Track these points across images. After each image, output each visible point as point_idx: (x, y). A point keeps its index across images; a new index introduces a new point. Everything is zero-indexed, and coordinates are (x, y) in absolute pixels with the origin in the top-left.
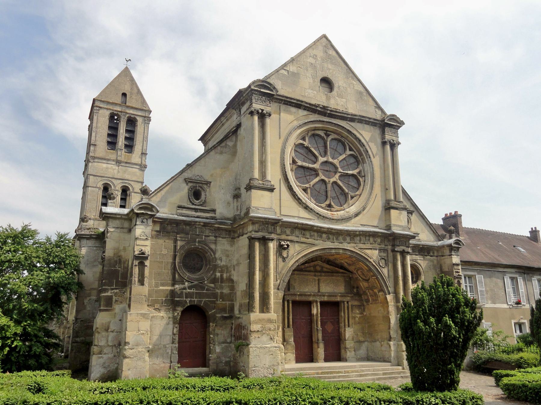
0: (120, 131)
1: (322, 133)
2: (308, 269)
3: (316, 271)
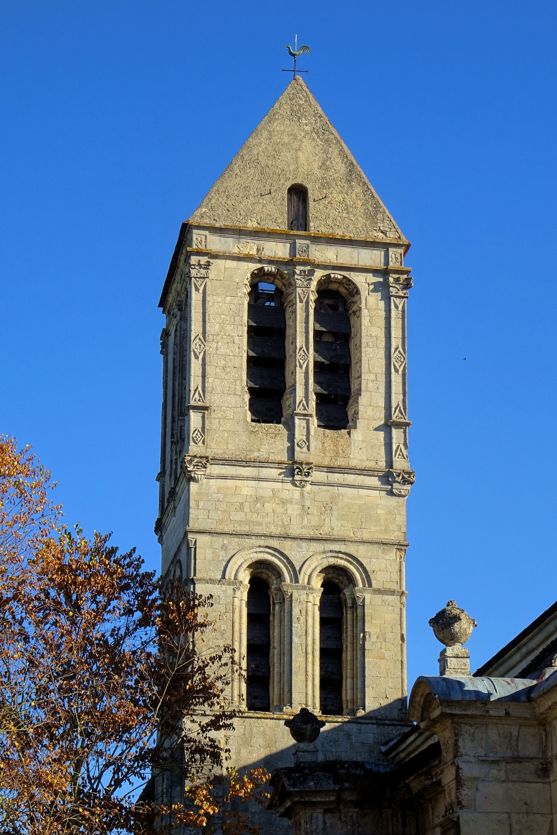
0: (294, 342)
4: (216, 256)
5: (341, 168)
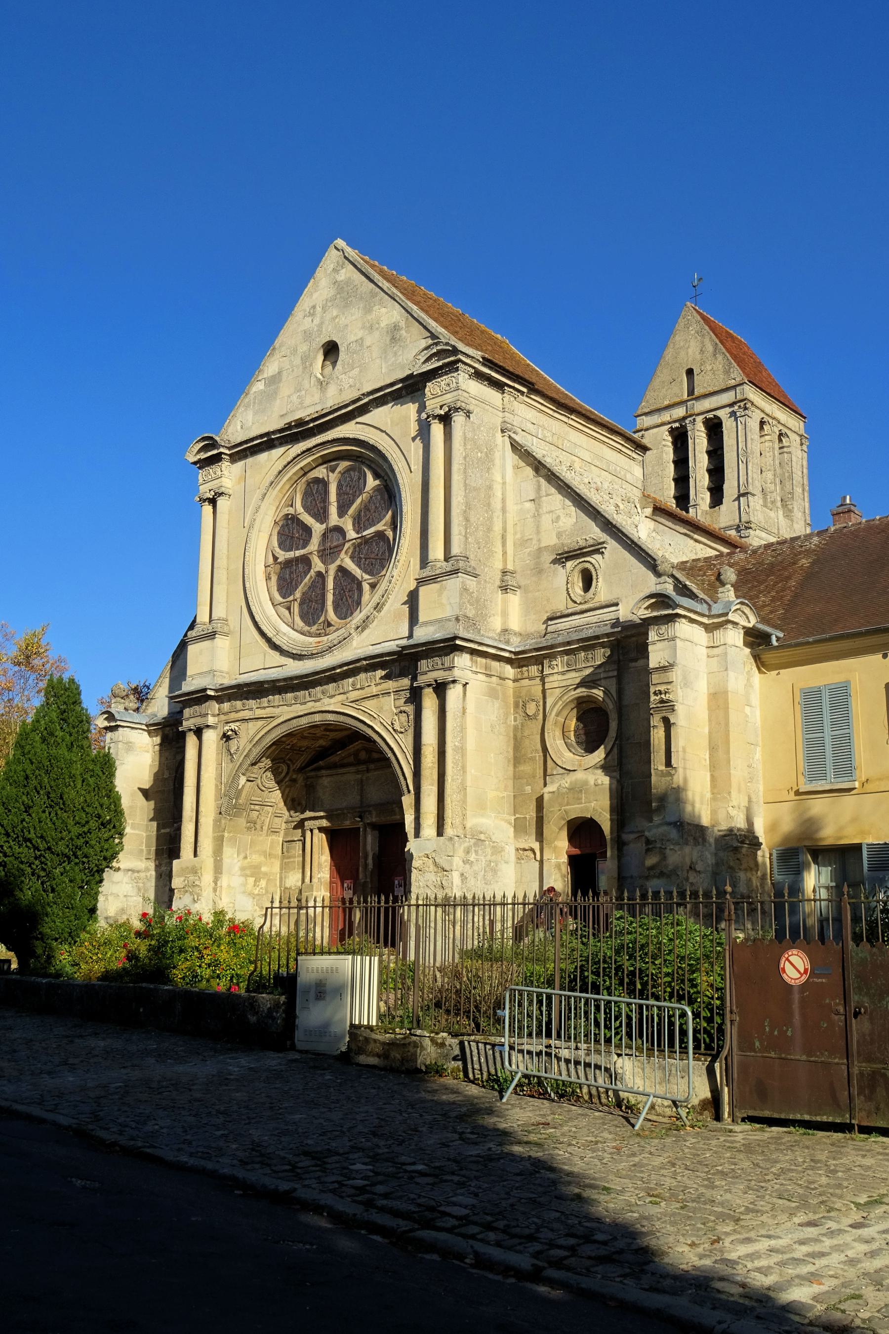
1: (321, 472)
2: (345, 761)
3: (359, 762)
4: (647, 430)
5: (710, 348)
